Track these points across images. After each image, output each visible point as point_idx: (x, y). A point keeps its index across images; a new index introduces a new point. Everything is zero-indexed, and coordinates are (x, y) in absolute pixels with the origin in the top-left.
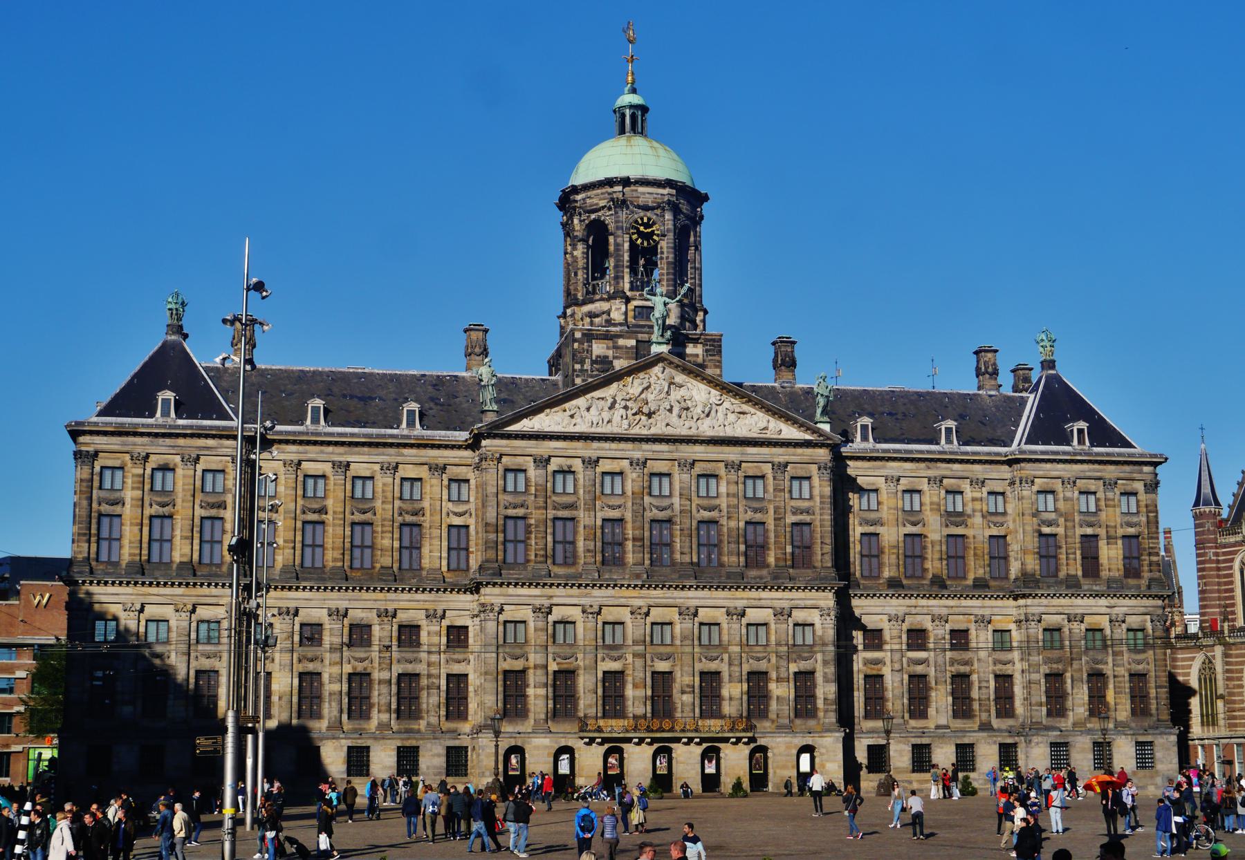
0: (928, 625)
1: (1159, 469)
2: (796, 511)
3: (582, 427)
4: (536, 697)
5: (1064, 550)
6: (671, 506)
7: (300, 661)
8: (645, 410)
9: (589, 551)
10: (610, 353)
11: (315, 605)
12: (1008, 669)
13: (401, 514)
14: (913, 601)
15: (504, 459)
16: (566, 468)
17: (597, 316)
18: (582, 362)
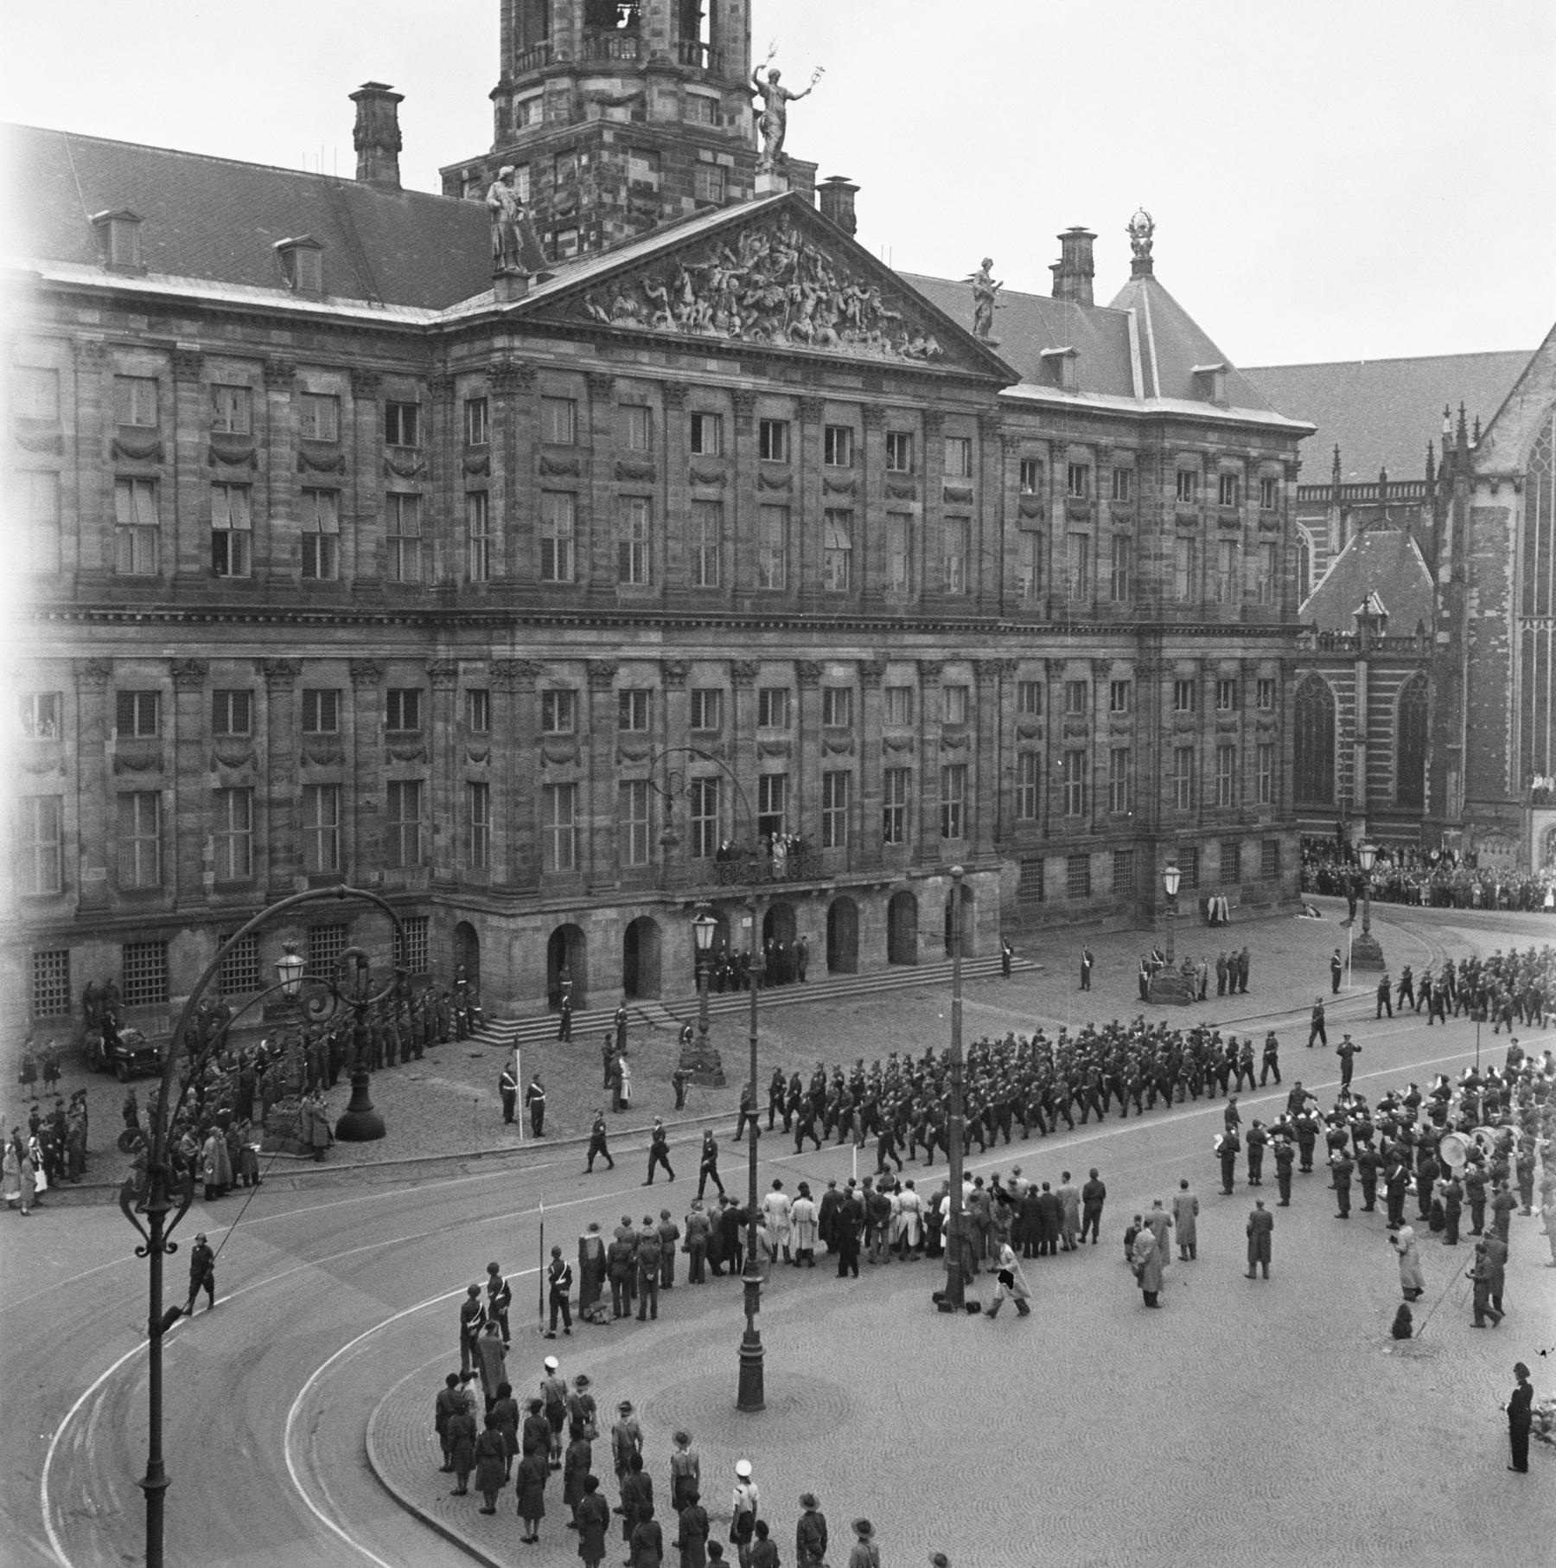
0: (1041, 677)
1: (1304, 444)
2: (951, 496)
4: (593, 831)
5: (1200, 562)
6: (787, 484)
7: (117, 771)
9: (674, 558)
10: (653, 178)
12: (1125, 740)
13: (301, 469)
14: (1028, 640)
15: (541, 375)
16: (637, 401)
17: (618, 103)
18: (614, 192)
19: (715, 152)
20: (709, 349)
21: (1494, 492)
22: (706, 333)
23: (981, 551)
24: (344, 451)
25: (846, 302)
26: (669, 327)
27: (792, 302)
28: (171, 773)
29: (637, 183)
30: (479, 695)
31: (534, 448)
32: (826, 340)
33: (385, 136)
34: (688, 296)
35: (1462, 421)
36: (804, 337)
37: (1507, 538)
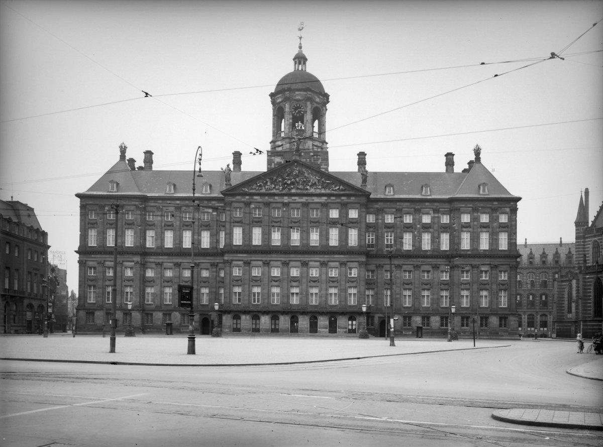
3: (263, 191)
8: (289, 182)
9: (266, 239)
11: (167, 261)
18: (271, 165)
22: (272, 191)
27: (298, 182)
29: (278, 162)
32: (307, 189)
34: (269, 184)
36: (301, 189)
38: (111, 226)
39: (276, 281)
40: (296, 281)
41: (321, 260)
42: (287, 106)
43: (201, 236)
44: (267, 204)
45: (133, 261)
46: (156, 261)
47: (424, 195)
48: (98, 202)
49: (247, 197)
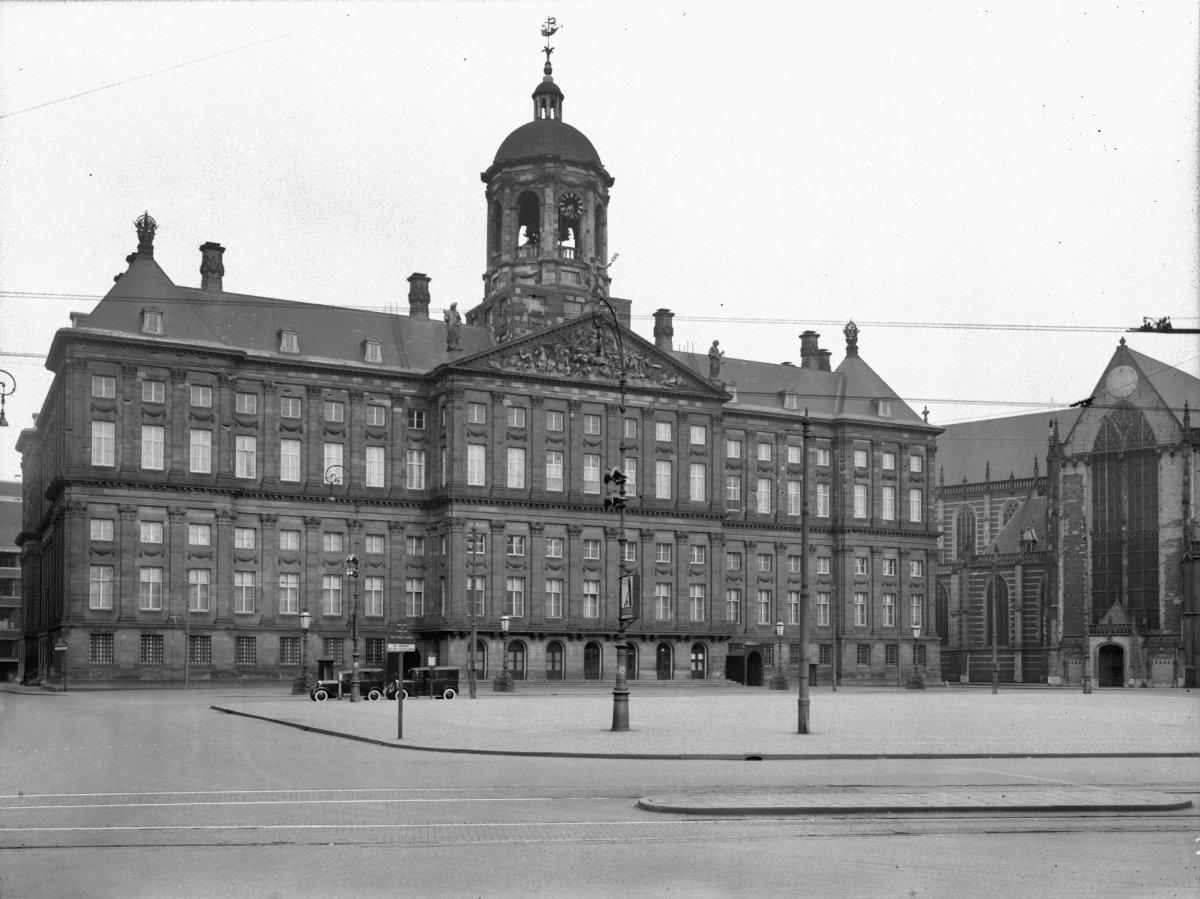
9: (536, 476)
10: (542, 309)
15: (468, 393)
16: (518, 405)
17: (529, 276)
19: (575, 296)
20: (554, 381)
21: (1075, 466)
22: (552, 375)
23: (712, 480)
24: (387, 430)
25: (630, 361)
26: (533, 371)
28: (304, 566)
30: (442, 536)
31: (463, 425)
33: (421, 297)
34: (543, 357)
35: (1056, 428)
36: (607, 376)
37: (1082, 491)
38: (152, 420)
39: (555, 569)
40: (594, 570)
41: (642, 526)
42: (549, 193)
43: (365, 459)
44: (536, 401)
45: (214, 510)
46: (265, 512)
47: (787, 410)
48: (119, 354)
49: (498, 382)
